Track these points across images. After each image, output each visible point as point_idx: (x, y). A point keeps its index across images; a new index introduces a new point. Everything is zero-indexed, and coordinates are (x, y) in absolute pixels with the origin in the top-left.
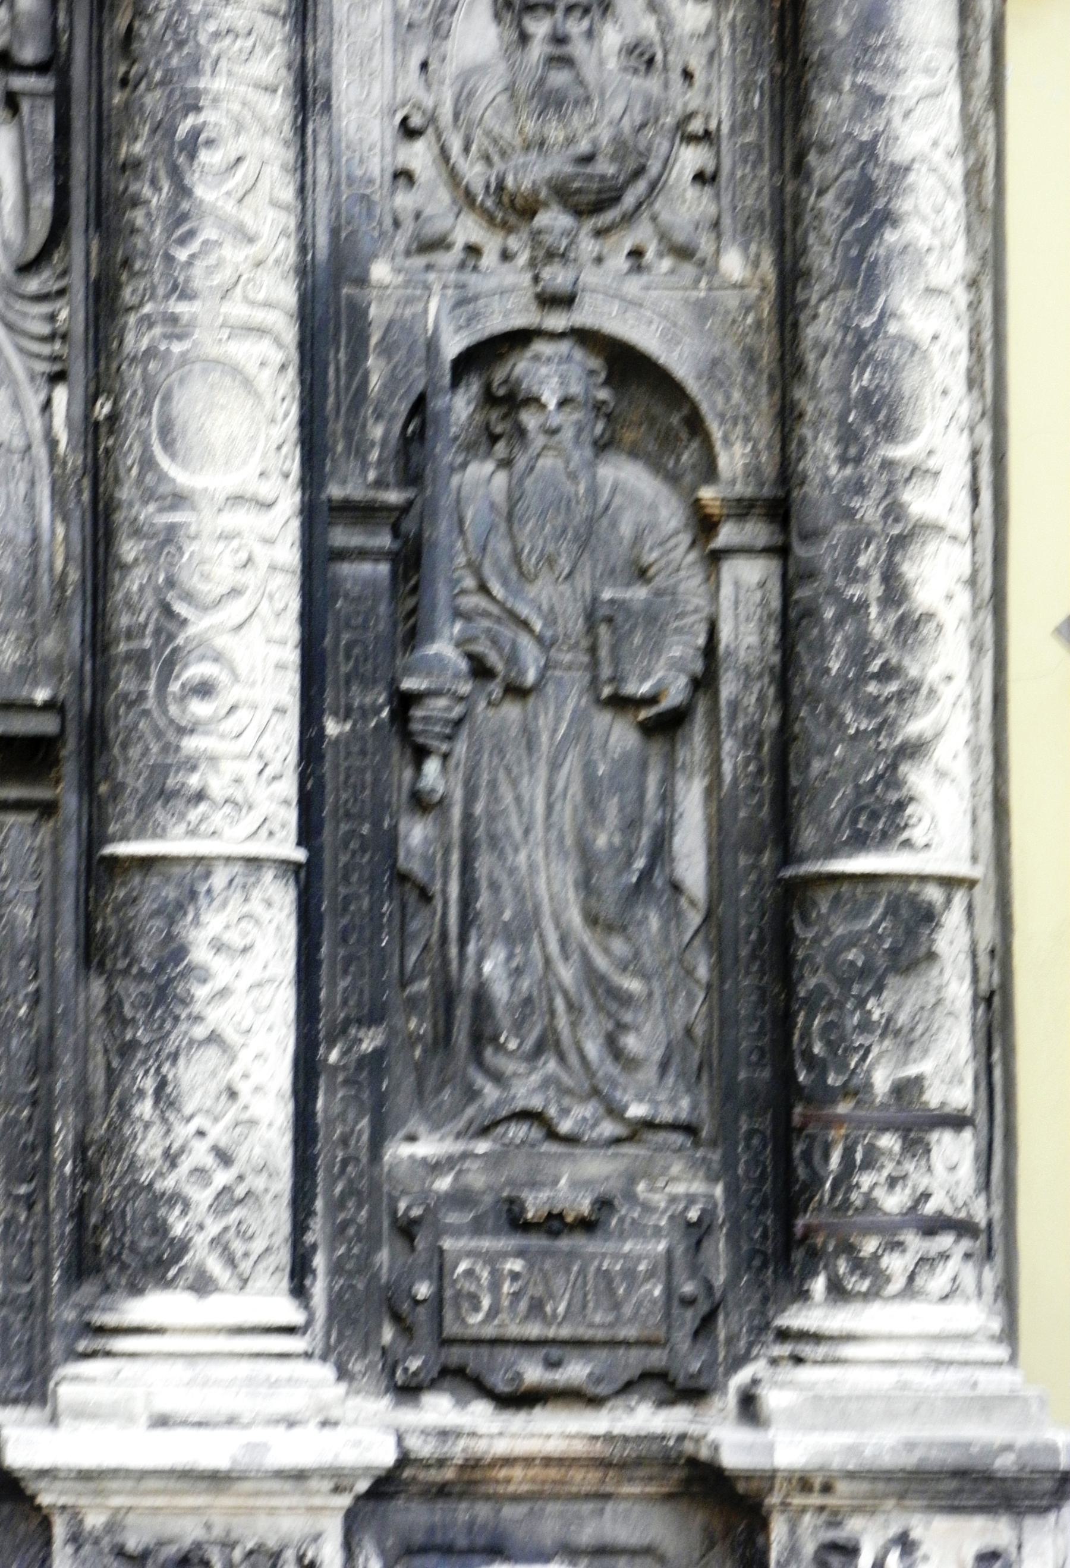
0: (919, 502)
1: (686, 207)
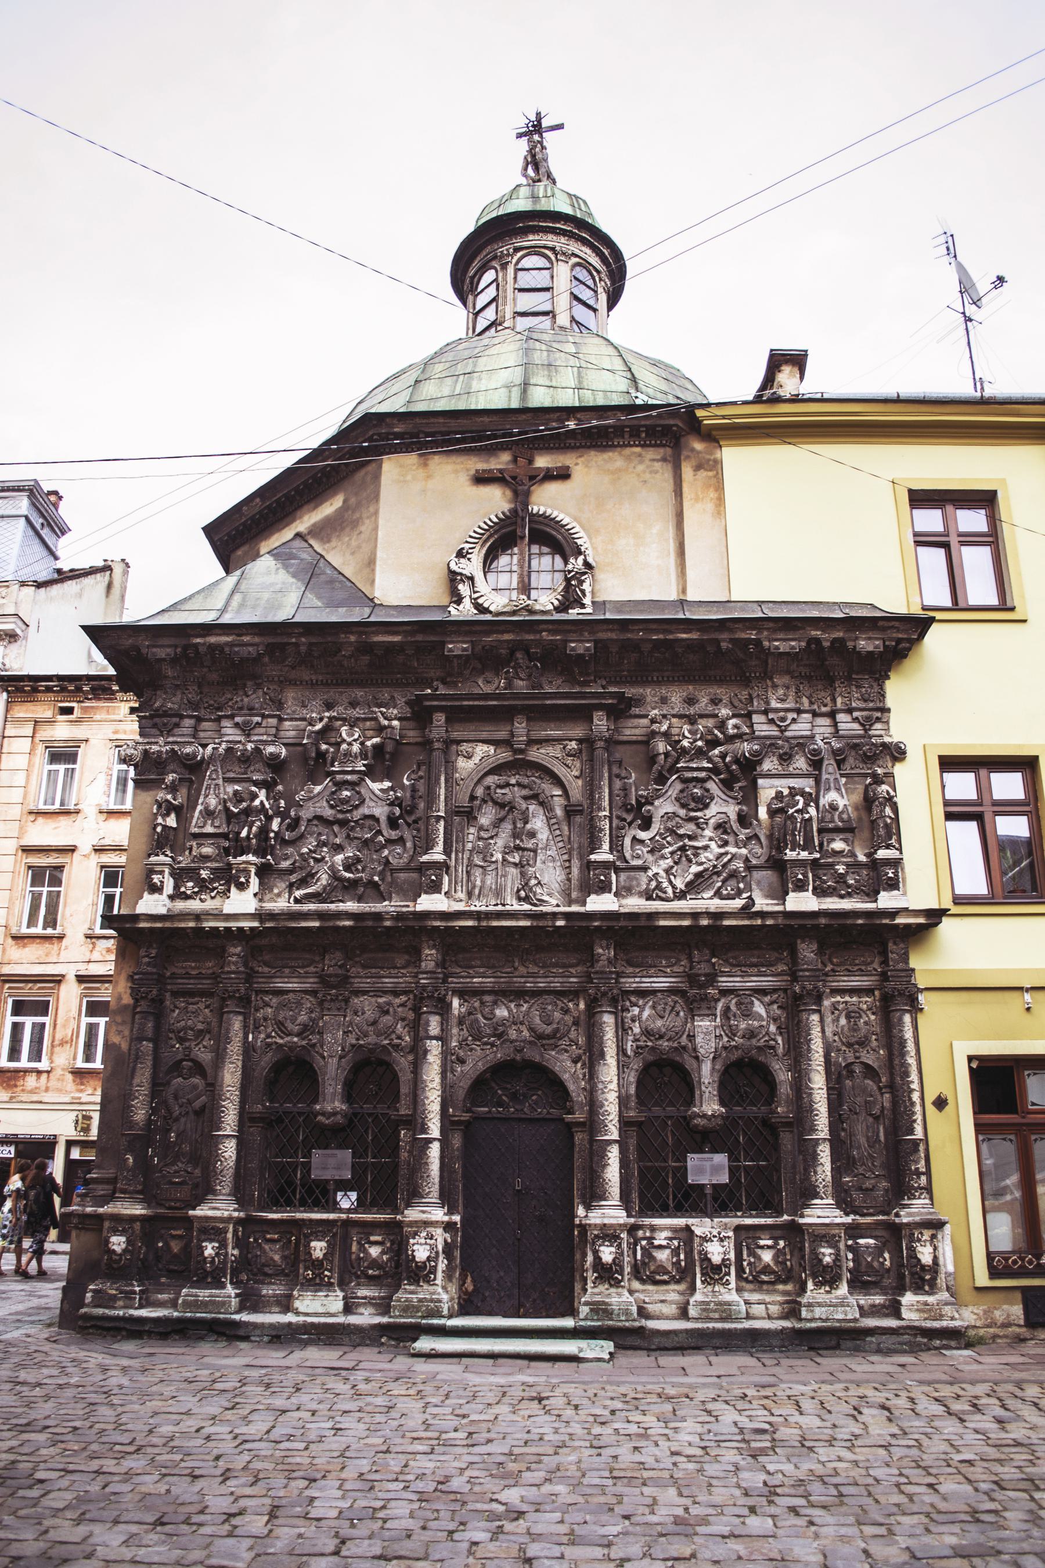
0: (913, 1086)
1: (874, 1044)
